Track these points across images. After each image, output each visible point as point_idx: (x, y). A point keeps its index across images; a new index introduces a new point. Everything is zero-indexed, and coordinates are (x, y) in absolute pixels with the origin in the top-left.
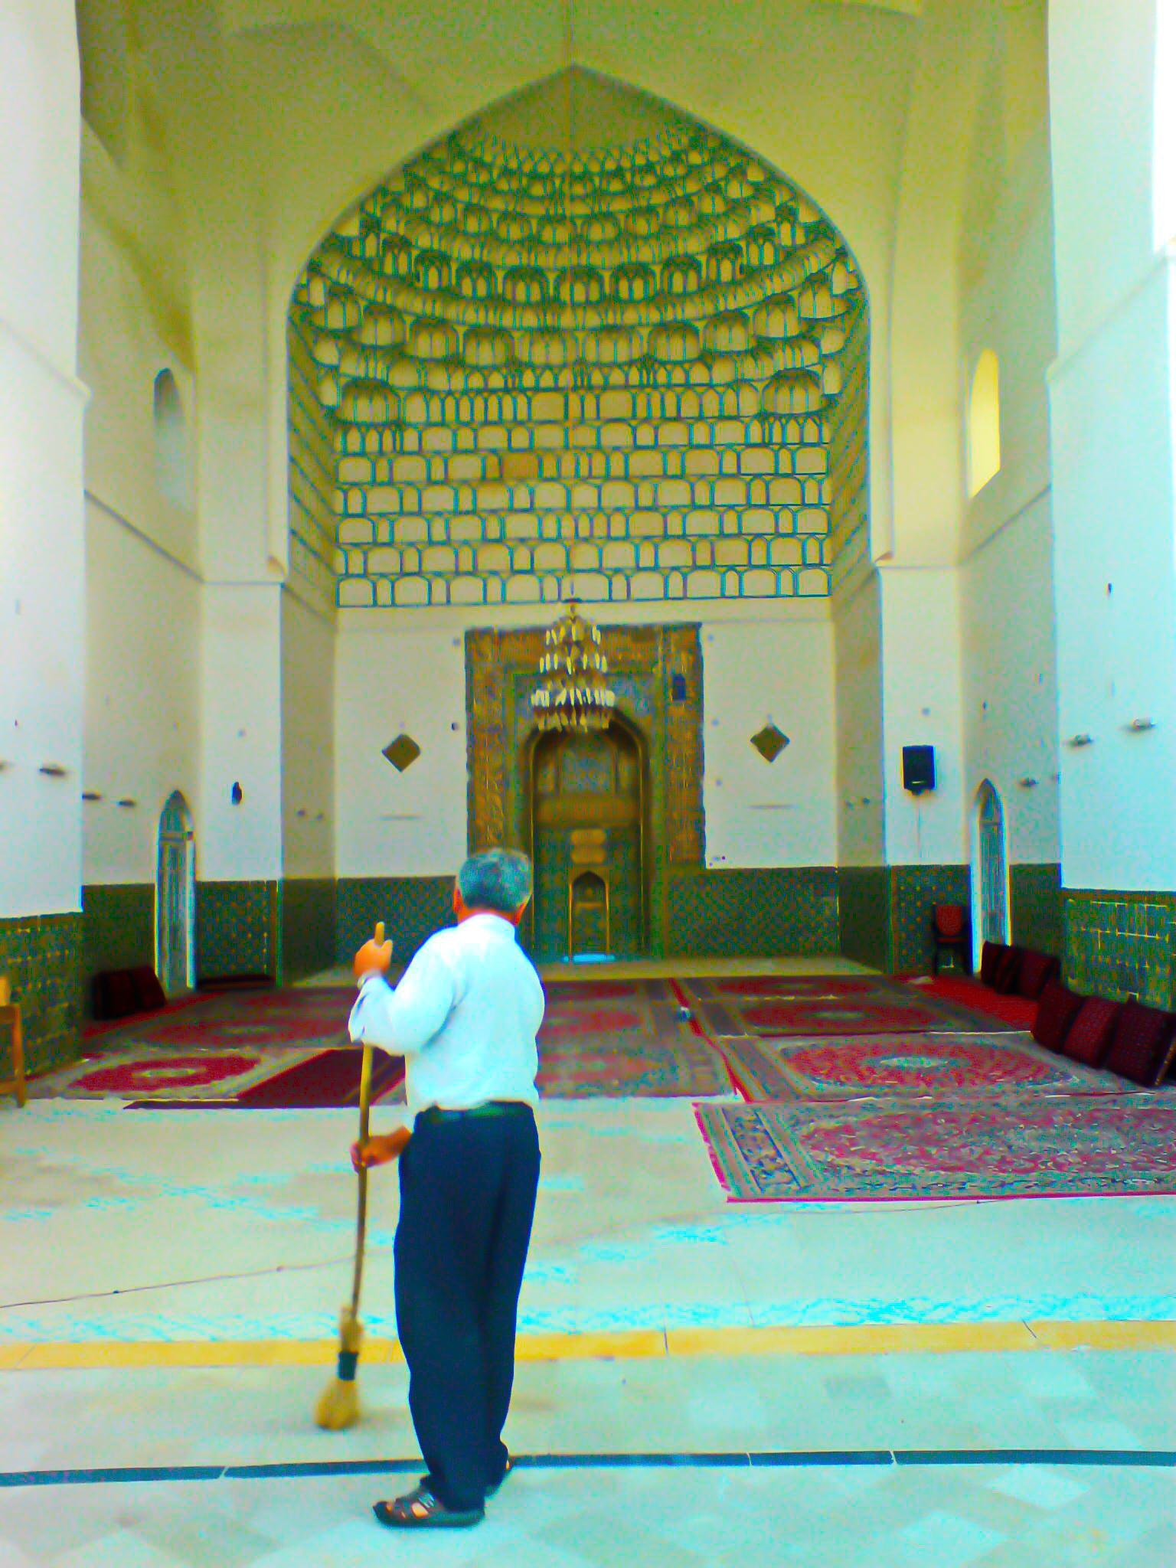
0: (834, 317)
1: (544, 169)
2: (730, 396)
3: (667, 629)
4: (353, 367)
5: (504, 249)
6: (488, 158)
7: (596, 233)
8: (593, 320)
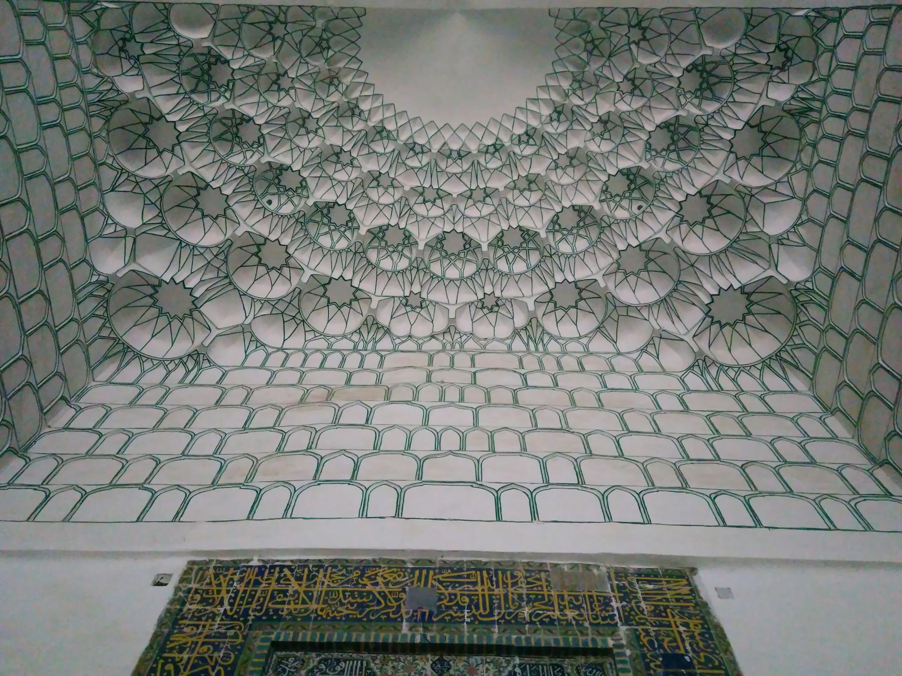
0: (778, 182)
1: (421, 141)
2: (647, 361)
3: (620, 574)
4: (155, 264)
5: (374, 212)
6: (365, 106)
7: (473, 212)
8: (467, 296)
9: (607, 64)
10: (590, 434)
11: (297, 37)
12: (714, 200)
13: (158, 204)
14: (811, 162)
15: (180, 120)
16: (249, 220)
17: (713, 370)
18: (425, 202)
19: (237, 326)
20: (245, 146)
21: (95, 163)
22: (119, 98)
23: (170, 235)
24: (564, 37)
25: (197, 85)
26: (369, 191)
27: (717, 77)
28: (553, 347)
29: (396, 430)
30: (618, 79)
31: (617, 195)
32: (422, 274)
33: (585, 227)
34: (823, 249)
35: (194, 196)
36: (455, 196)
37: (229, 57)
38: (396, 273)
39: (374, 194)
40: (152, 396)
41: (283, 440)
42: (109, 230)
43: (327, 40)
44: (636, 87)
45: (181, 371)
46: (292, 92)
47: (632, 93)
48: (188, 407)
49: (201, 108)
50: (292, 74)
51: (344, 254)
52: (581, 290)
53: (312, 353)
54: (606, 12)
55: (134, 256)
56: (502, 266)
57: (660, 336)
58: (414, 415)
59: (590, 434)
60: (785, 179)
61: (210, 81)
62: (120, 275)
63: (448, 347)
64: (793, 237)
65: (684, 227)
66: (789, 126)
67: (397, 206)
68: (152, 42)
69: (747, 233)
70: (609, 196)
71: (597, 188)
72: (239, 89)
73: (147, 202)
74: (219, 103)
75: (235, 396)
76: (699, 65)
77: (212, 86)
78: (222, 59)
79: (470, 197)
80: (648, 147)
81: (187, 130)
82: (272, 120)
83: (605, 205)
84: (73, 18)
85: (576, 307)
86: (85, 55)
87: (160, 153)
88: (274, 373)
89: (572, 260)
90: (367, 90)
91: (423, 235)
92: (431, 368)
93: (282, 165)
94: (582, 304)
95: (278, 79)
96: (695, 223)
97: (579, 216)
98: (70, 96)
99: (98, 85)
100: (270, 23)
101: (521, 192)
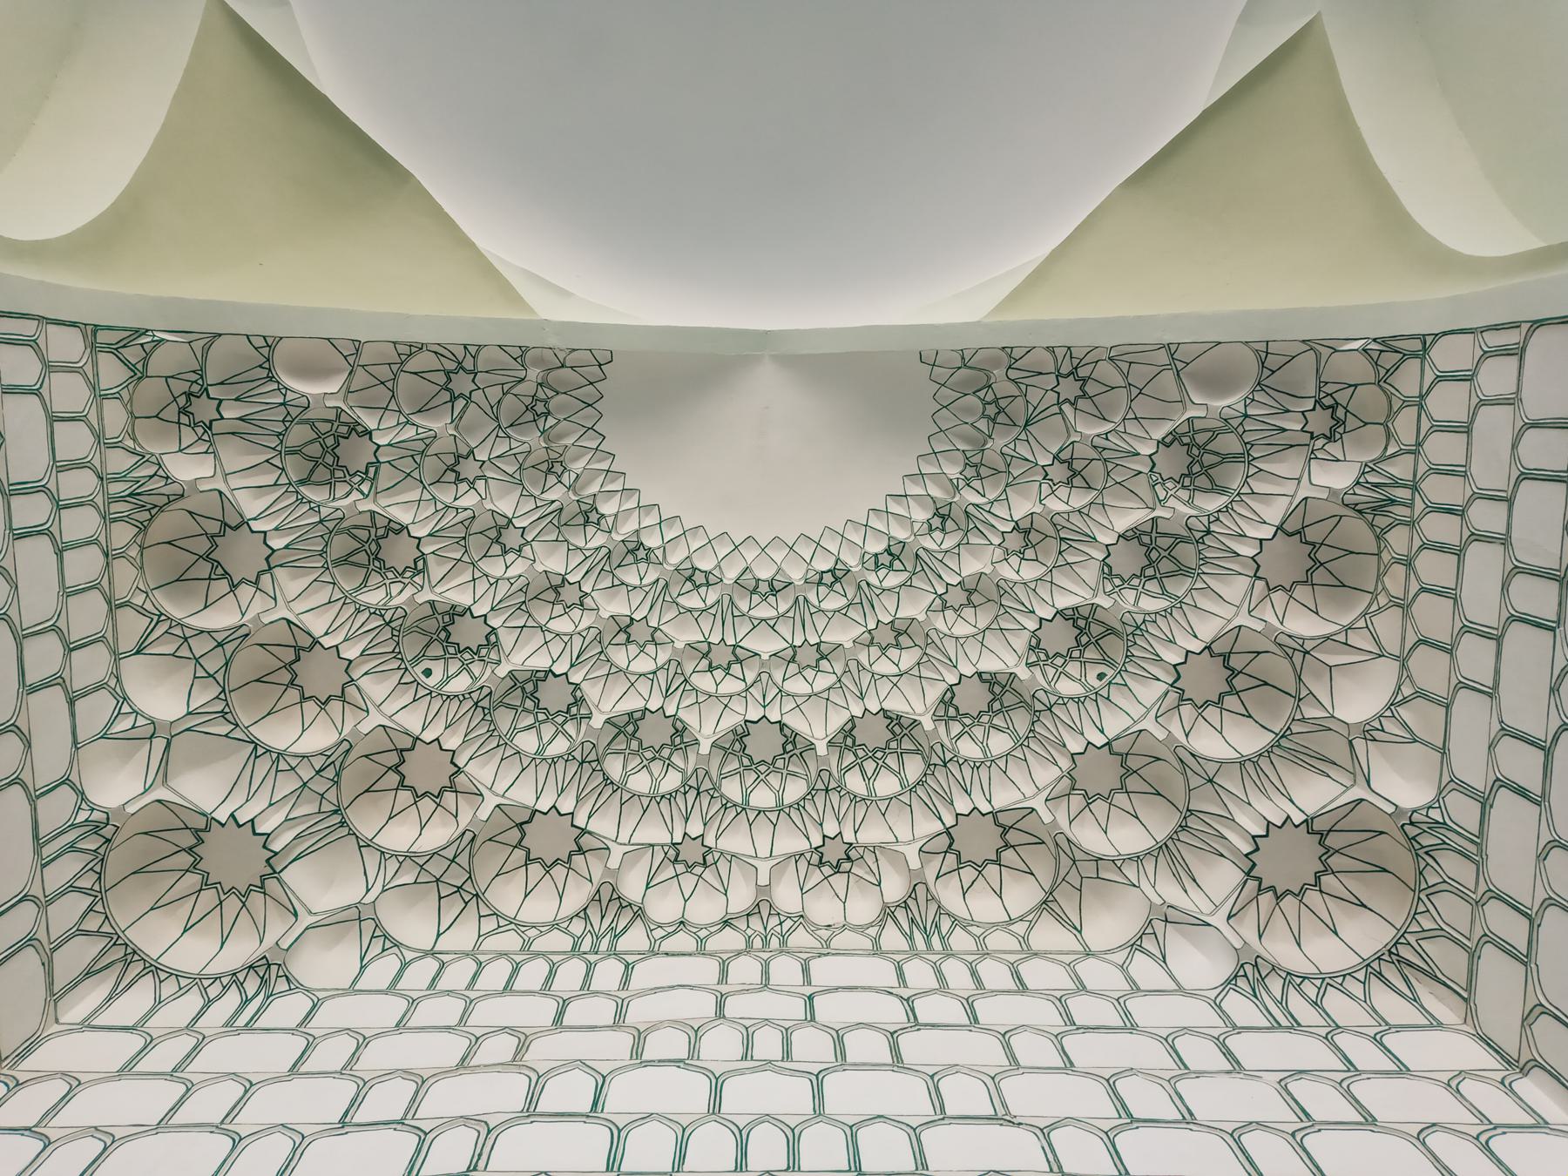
0: (1347, 629)
1: (705, 564)
2: (1144, 969)
4: (203, 788)
6: (608, 508)
7: (797, 686)
8: (790, 842)
9: (1023, 436)
10: (1053, 1126)
11: (494, 394)
12: (1236, 662)
13: (219, 677)
14: (1406, 591)
15: (276, 529)
16: (387, 704)
17: (1275, 985)
18: (711, 668)
19: (349, 907)
20: (390, 575)
21: (109, 603)
22: (165, 490)
23: (238, 734)
24: (947, 394)
25: (312, 471)
26: (611, 651)
27: (1217, 454)
28: (960, 941)
29: (653, 1126)
30: (1044, 460)
31: (1057, 655)
32: (705, 799)
33: (1004, 710)
34: (1453, 746)
35: (289, 664)
36: (765, 657)
37: (372, 425)
38: (656, 798)
39: (620, 657)
40: (166, 1055)
41: (418, 1151)
42: (124, 724)
43: (546, 402)
44: (1075, 474)
45: (233, 999)
46: (480, 484)
47: (1069, 483)
48: (234, 1076)
49: (315, 508)
50: (482, 455)
51: (560, 765)
52: (1005, 830)
53: (490, 961)
54: (1017, 354)
55: (164, 774)
56: (855, 782)
57: (1164, 917)
58: (690, 1093)
59: (1053, 1126)
60: (1361, 623)
61: (338, 464)
62: (131, 809)
63: (758, 943)
64: (1390, 726)
65: (1187, 710)
66: (1356, 531)
67: (661, 675)
68: (237, 399)
69: (1303, 720)
70: (1043, 657)
71: (1020, 642)
72: (386, 477)
73: (200, 673)
74: (351, 502)
75: (332, 1054)
76: (1184, 434)
77: (339, 474)
78: (360, 429)
79: (793, 660)
80: (1107, 572)
81: (286, 547)
82: (441, 530)
83: (1037, 671)
84: (101, 355)
85: (998, 862)
86: (115, 417)
87: (234, 587)
88: (413, 1003)
89: (984, 772)
90: (613, 481)
91: (708, 729)
92: (724, 989)
93: (453, 607)
94: (1009, 856)
95: (457, 462)
96: (1207, 703)
97: (992, 692)
98: (79, 484)
99: (131, 470)
100: (448, 373)
101: (883, 650)
